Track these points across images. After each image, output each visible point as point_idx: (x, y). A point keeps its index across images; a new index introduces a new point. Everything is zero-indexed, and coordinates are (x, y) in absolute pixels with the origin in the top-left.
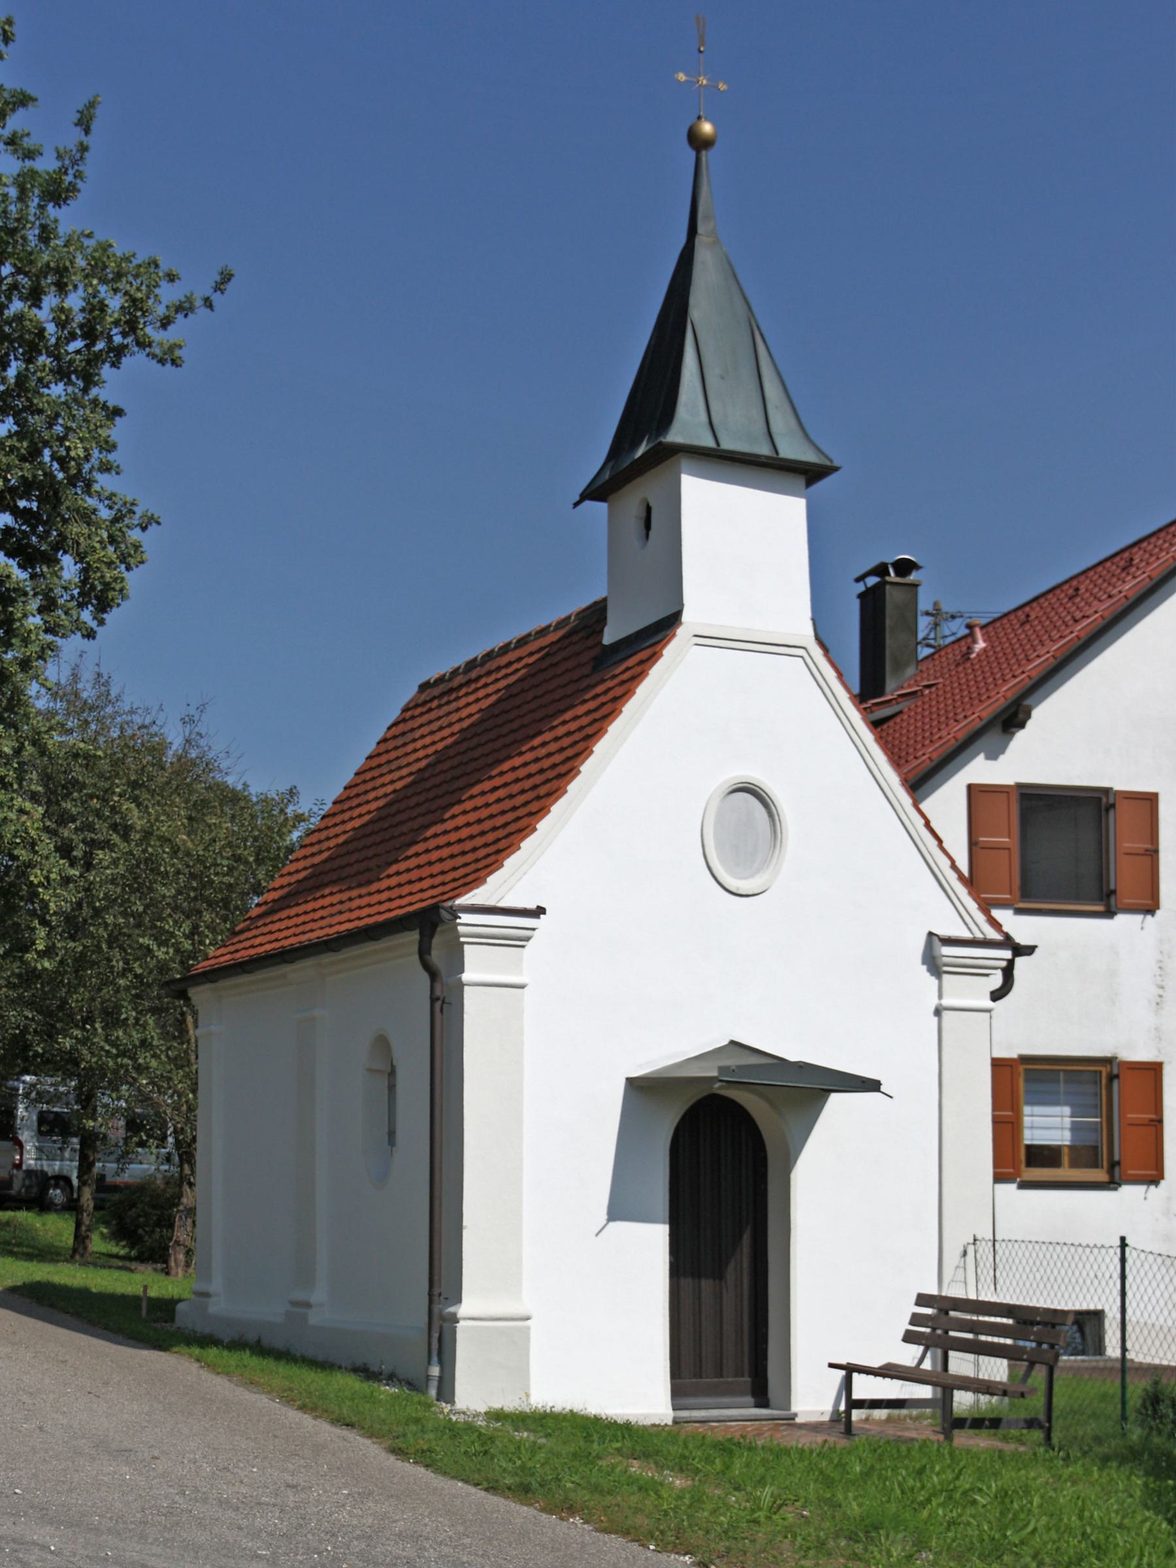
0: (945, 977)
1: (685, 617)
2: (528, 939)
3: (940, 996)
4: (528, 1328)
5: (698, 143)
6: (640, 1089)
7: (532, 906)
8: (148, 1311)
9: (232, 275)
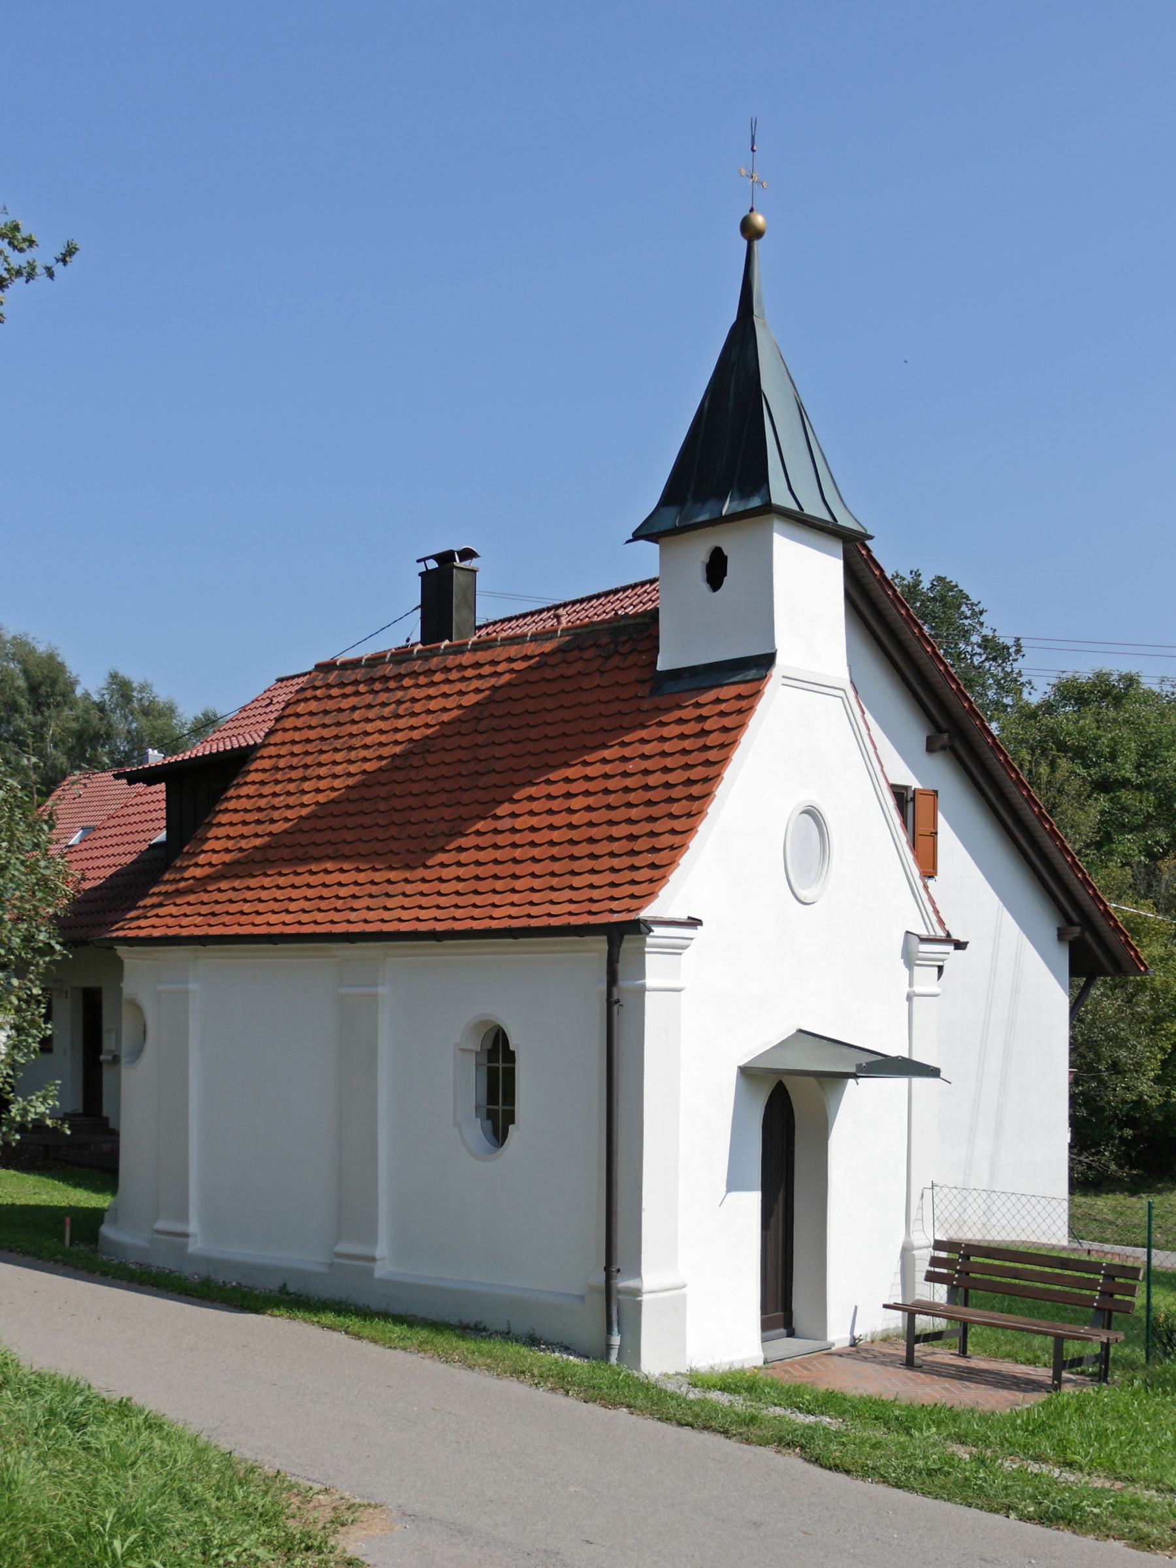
0: (916, 968)
1: (779, 660)
2: (685, 947)
3: (911, 984)
4: (685, 1296)
5: (750, 232)
6: (746, 1073)
7: (682, 916)
8: (71, 1242)
9: (76, 249)
